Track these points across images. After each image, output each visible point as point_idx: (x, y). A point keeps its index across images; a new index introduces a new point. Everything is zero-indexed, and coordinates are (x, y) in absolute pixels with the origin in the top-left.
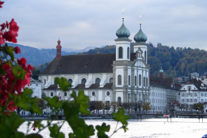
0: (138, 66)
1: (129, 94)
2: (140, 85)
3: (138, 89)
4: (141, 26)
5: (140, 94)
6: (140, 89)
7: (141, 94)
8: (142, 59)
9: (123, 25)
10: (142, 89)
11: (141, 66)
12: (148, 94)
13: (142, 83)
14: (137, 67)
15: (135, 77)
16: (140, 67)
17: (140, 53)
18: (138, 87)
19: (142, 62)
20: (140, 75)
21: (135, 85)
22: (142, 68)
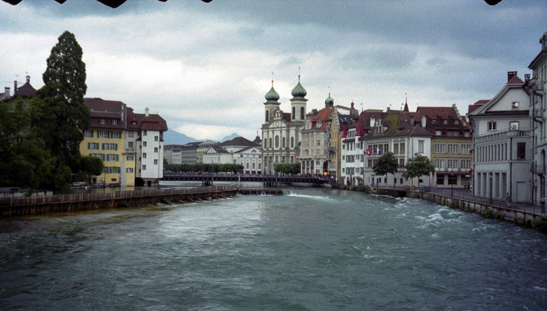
0: (275, 126)
1: (266, 158)
2: (277, 146)
3: (273, 151)
4: (299, 79)
5: (277, 157)
6: (277, 151)
7: (279, 156)
8: (280, 118)
9: (272, 88)
10: (281, 150)
11: (280, 126)
12: (293, 155)
13: (281, 144)
14: (274, 128)
15: (271, 139)
16: (277, 128)
17: (278, 113)
18: (273, 149)
19: (280, 122)
20: (277, 137)
21: (270, 147)
22: (281, 127)
